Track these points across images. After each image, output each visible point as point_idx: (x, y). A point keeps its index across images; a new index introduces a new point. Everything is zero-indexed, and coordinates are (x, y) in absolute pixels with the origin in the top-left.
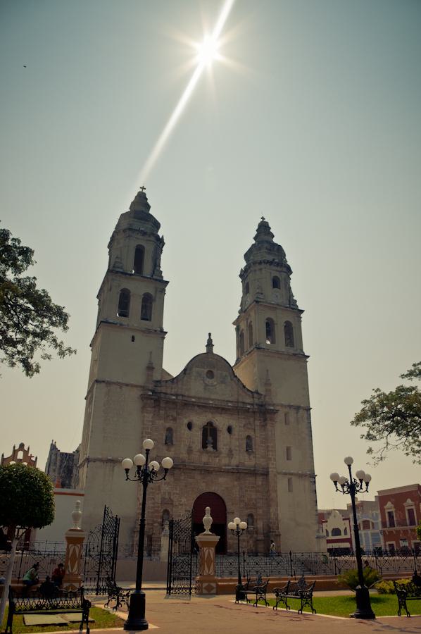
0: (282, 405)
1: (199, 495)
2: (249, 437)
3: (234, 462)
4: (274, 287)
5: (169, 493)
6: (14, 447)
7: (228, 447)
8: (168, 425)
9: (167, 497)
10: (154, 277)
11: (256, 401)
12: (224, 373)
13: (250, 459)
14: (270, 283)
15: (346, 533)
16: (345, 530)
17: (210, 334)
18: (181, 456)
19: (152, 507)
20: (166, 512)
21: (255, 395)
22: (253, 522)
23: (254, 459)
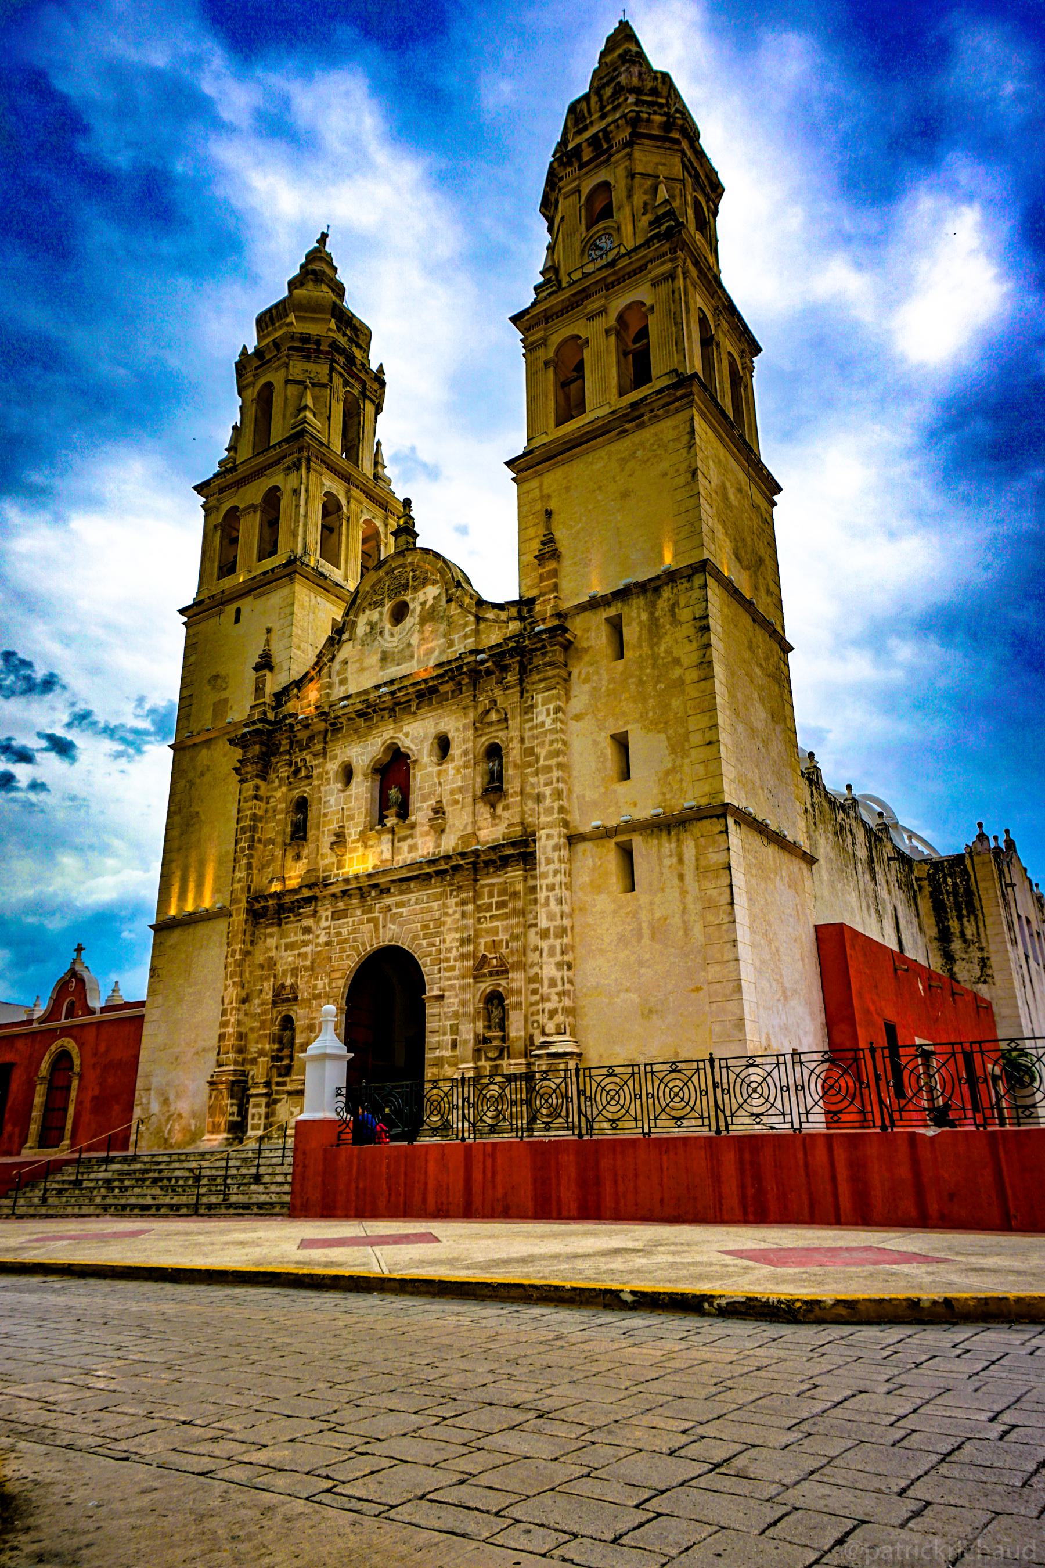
0: (594, 604)
3: (449, 843)
7: (432, 802)
8: (296, 794)
9: (289, 982)
13: (494, 816)
23: (506, 814)
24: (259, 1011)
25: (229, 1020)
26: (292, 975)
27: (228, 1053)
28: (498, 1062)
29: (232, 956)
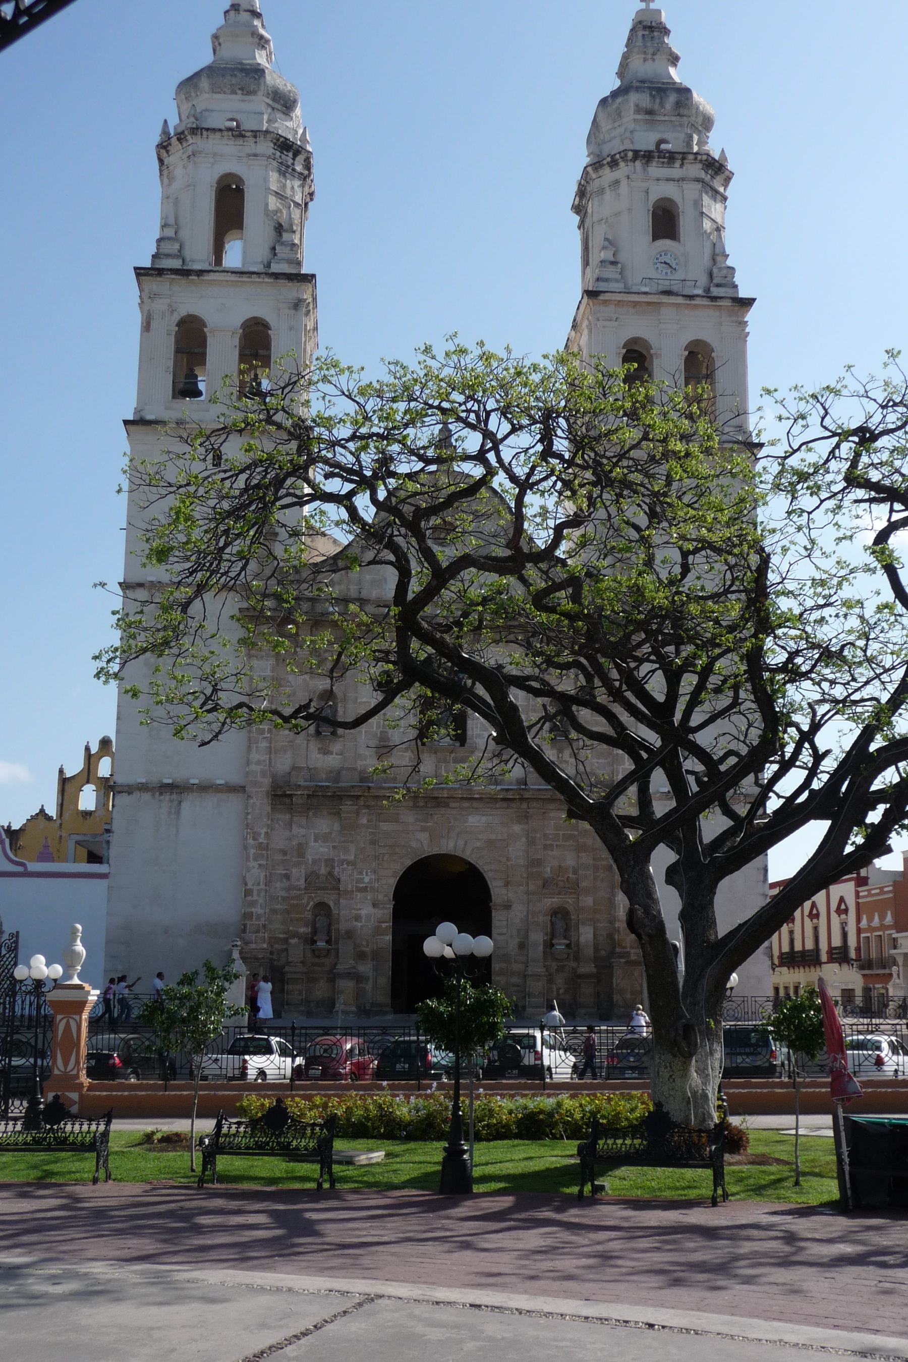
1: (409, 863)
4: (656, 236)
5: (329, 862)
6: (87, 749)
9: (323, 871)
10: (275, 268)
14: (645, 223)
18: (360, 764)
19: (283, 898)
20: (322, 908)
22: (567, 929)
24: (283, 894)
25: (256, 901)
26: (326, 866)
27: (258, 932)
28: (566, 963)
29: (254, 839)
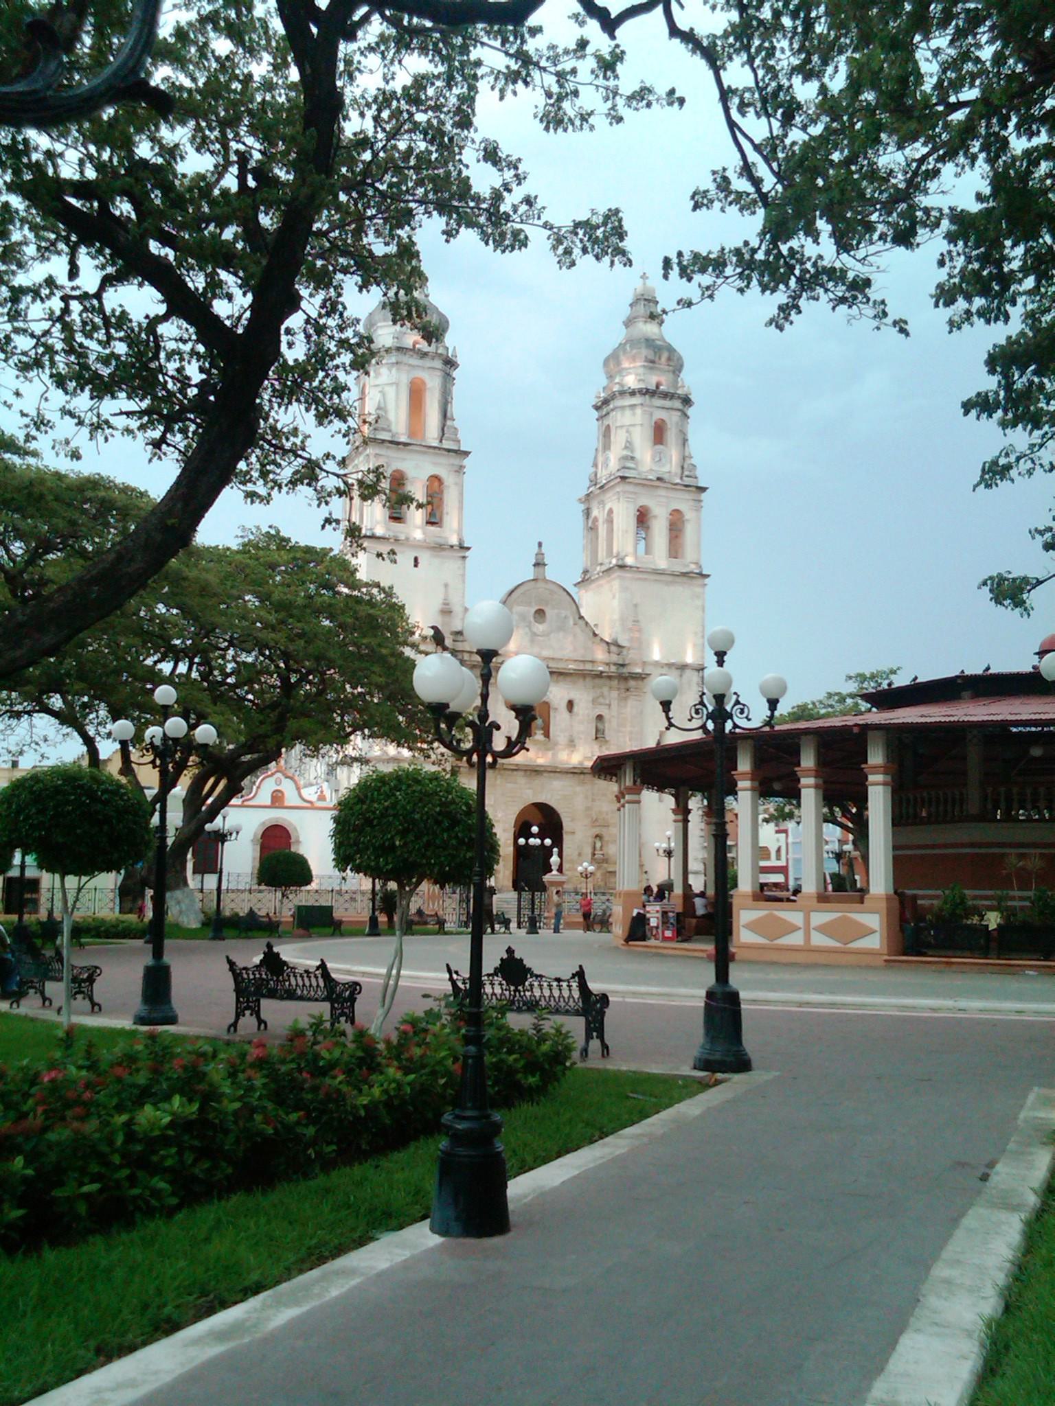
2: (600, 717)
11: (614, 658)
12: (564, 613)
15: (778, 858)
16: (779, 850)
17: (540, 545)
21: (613, 648)
